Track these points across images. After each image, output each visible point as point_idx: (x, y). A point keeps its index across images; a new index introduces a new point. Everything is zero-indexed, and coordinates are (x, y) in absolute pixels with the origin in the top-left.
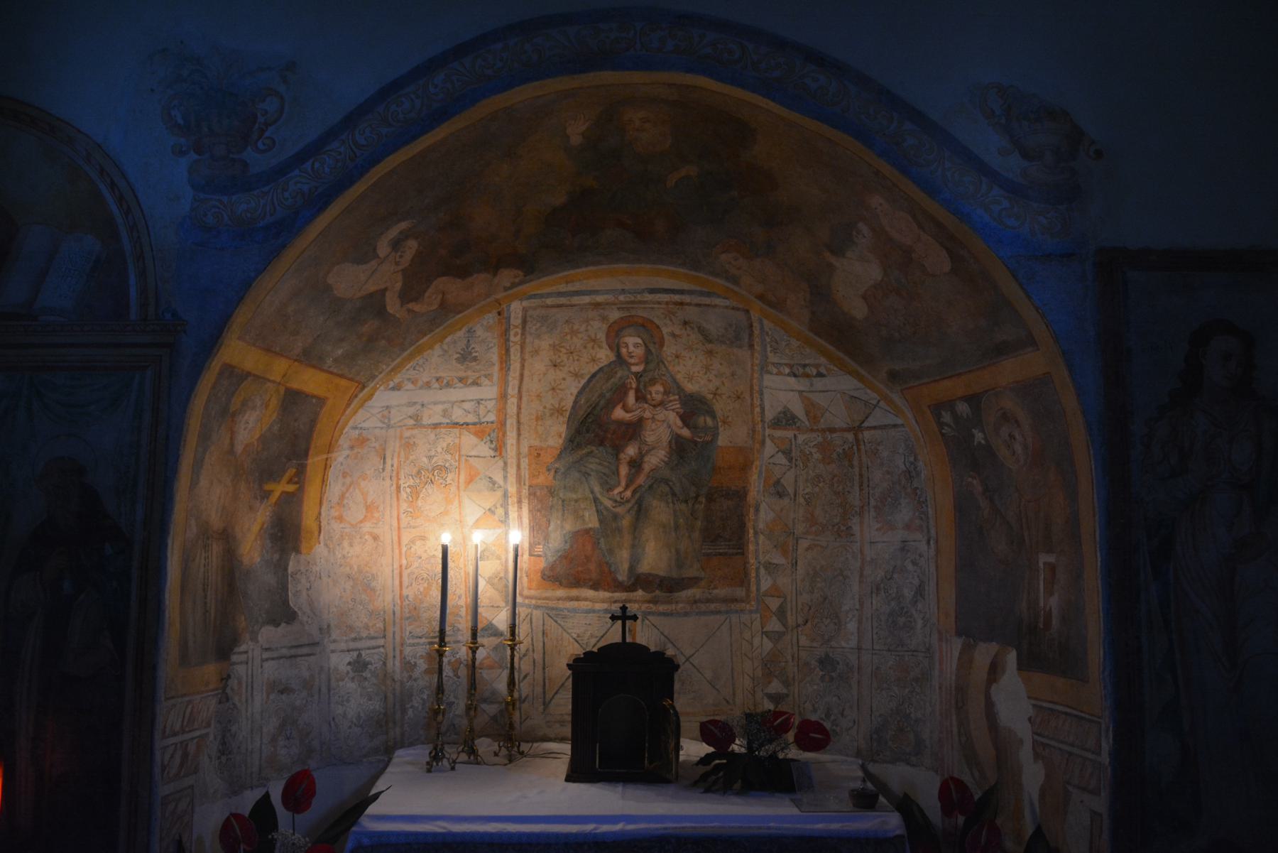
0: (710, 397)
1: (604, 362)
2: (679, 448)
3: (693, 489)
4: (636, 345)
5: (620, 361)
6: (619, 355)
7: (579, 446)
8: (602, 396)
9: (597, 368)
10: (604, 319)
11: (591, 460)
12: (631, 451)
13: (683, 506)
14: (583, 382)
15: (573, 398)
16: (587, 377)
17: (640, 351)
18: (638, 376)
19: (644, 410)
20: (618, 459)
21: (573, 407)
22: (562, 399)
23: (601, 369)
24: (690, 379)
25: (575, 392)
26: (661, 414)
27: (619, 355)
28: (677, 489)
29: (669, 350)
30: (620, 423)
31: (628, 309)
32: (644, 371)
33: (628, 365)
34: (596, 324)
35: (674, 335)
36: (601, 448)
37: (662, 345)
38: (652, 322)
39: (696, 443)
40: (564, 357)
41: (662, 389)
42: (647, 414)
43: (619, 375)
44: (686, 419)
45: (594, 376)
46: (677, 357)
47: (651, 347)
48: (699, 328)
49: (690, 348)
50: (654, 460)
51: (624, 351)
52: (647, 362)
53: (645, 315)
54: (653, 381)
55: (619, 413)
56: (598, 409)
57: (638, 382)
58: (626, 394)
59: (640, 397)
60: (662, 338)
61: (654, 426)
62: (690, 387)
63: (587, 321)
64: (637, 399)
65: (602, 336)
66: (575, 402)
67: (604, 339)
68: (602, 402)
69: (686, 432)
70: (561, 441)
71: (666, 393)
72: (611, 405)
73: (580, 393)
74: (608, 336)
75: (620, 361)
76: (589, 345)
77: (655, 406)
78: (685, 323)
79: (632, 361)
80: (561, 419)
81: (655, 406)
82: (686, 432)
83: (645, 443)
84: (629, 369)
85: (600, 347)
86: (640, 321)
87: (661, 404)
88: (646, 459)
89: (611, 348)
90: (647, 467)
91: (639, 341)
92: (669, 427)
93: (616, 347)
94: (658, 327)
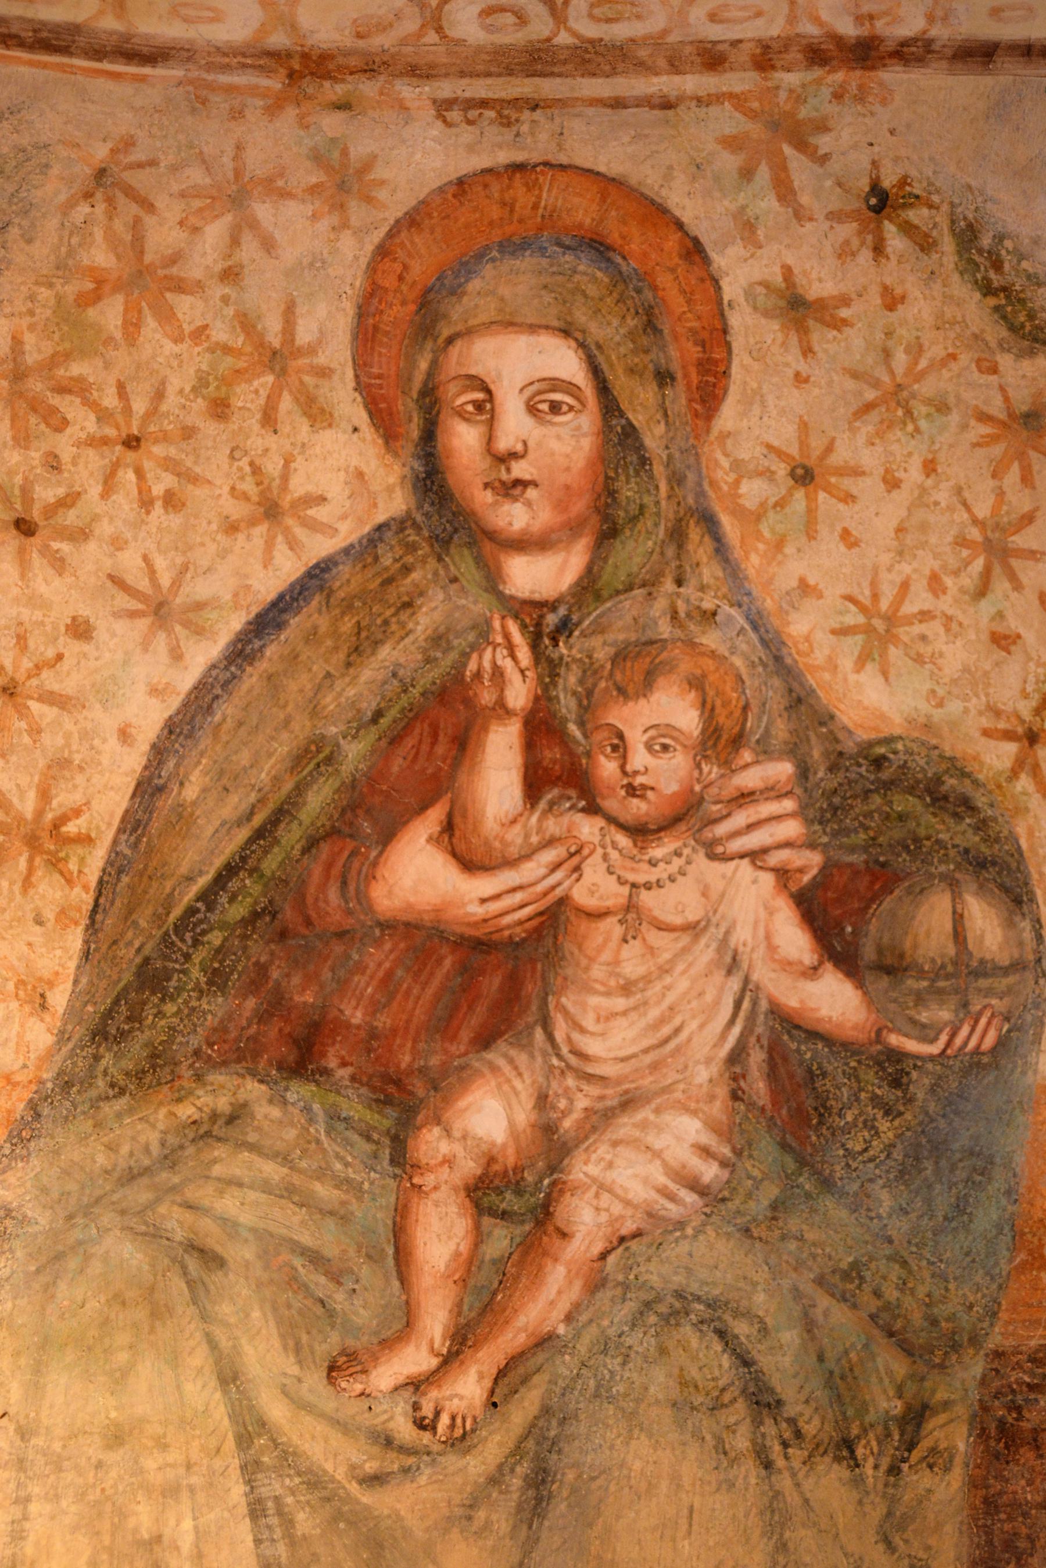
0: (998, 756)
1: (336, 528)
2: (794, 1095)
3: (890, 1363)
4: (545, 400)
5: (442, 518)
6: (432, 481)
7: (155, 1072)
8: (315, 756)
9: (288, 568)
10: (344, 183)
11: (228, 1162)
12: (489, 1115)
13: (828, 1484)
14: (203, 655)
15: (132, 762)
16: (234, 623)
17: (565, 446)
18: (545, 626)
19: (575, 858)
20: (401, 1156)
21: (133, 824)
22: (61, 765)
23: (316, 578)
24: (878, 632)
25: (150, 718)
26: (683, 884)
27: (432, 481)
28: (783, 1361)
29: (760, 417)
30: (423, 938)
31: (507, 112)
32: (589, 588)
33: (487, 545)
34: (294, 226)
35: (796, 308)
36: (298, 1091)
37: (709, 389)
38: (657, 214)
39: (895, 1068)
40: (87, 470)
41: (688, 719)
42: (596, 886)
43: (424, 621)
44: (835, 916)
45: (268, 621)
46: (804, 476)
47: (640, 402)
48: (967, 235)
49: (893, 403)
50: (641, 1170)
51: (464, 439)
52: (608, 524)
53: (611, 157)
54: (640, 665)
55: (417, 874)
56: (291, 836)
57: (548, 669)
58: (464, 744)
59: (556, 772)
60: (715, 337)
61: (633, 966)
62: (873, 700)
63: (236, 194)
64: (535, 783)
65: (327, 326)
66: (149, 789)
67: (338, 352)
68: (318, 800)
69: (834, 1000)
70: (40, 1035)
71: (721, 741)
72: (368, 817)
73: (181, 729)
74: (366, 335)
75: (442, 518)
76: (251, 396)
77: (641, 832)
78: (881, 202)
79: (515, 517)
80: (50, 891)
81: (641, 832)
82: (834, 1000)
83: (580, 1066)
84: (492, 580)
85: (318, 414)
86: (582, 209)
87: (685, 814)
88: (583, 1168)
89: (383, 419)
90: (586, 1221)
91: (565, 362)
92: (732, 963)
93: (414, 415)
94: (695, 251)
